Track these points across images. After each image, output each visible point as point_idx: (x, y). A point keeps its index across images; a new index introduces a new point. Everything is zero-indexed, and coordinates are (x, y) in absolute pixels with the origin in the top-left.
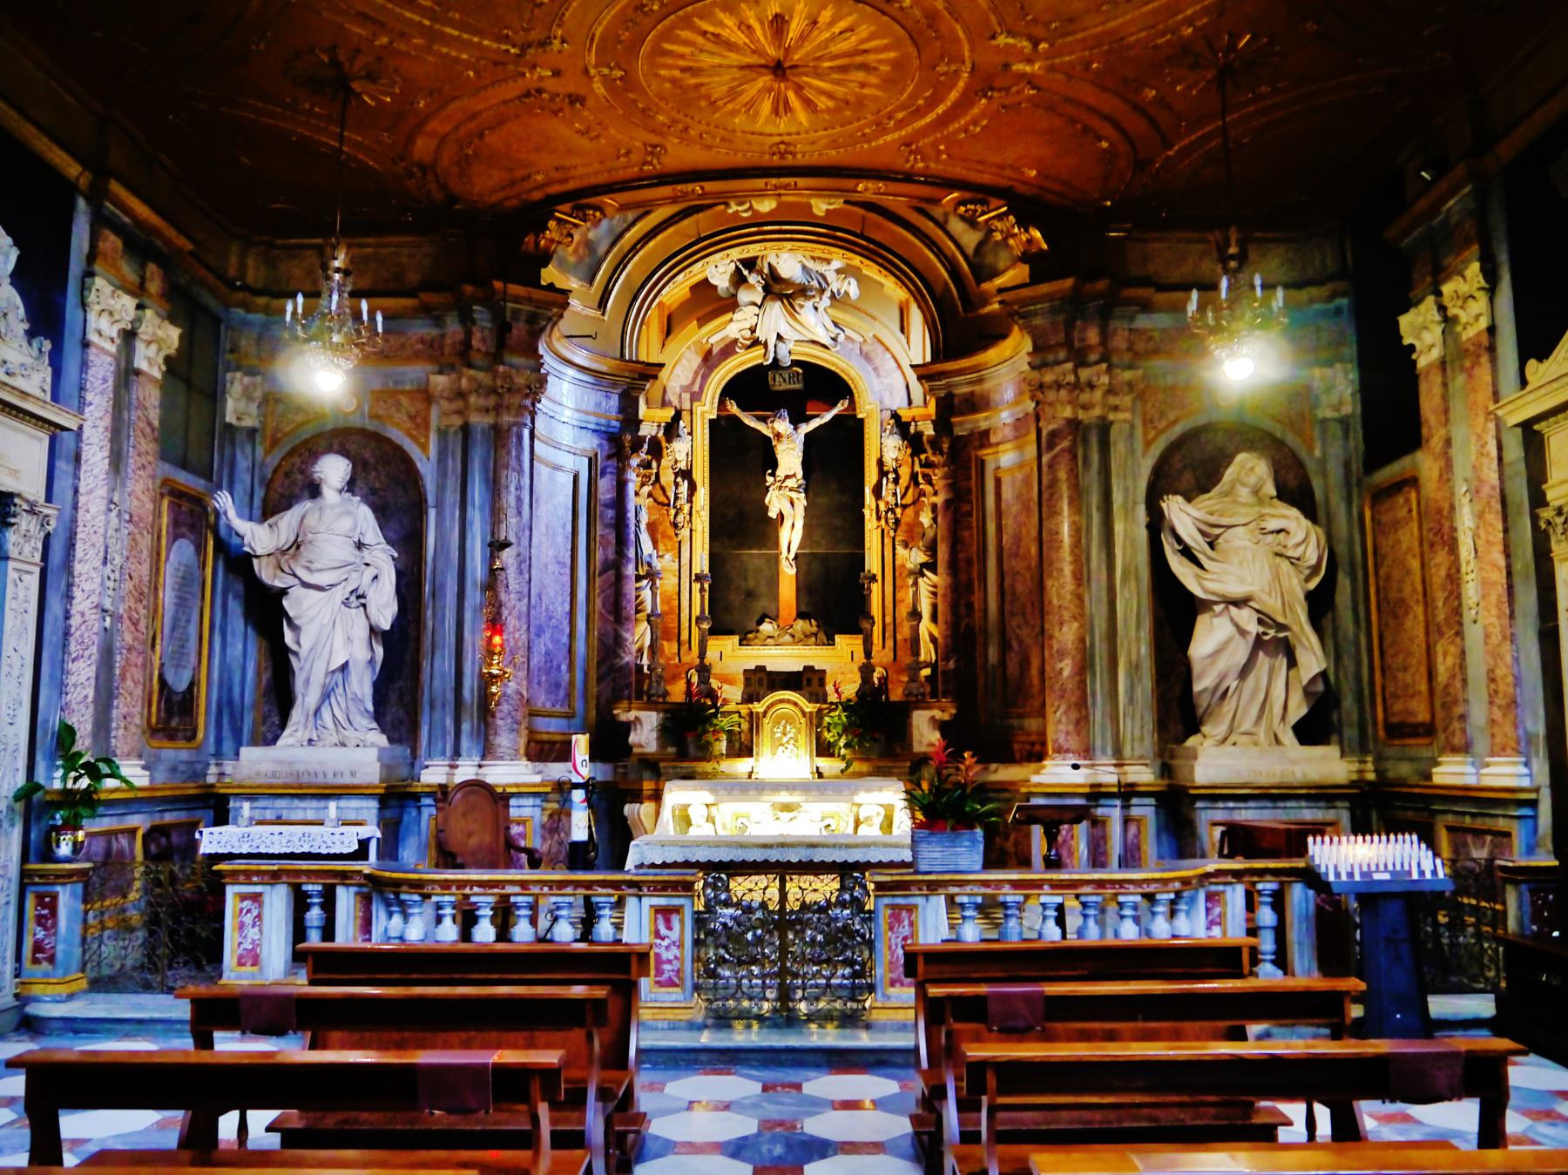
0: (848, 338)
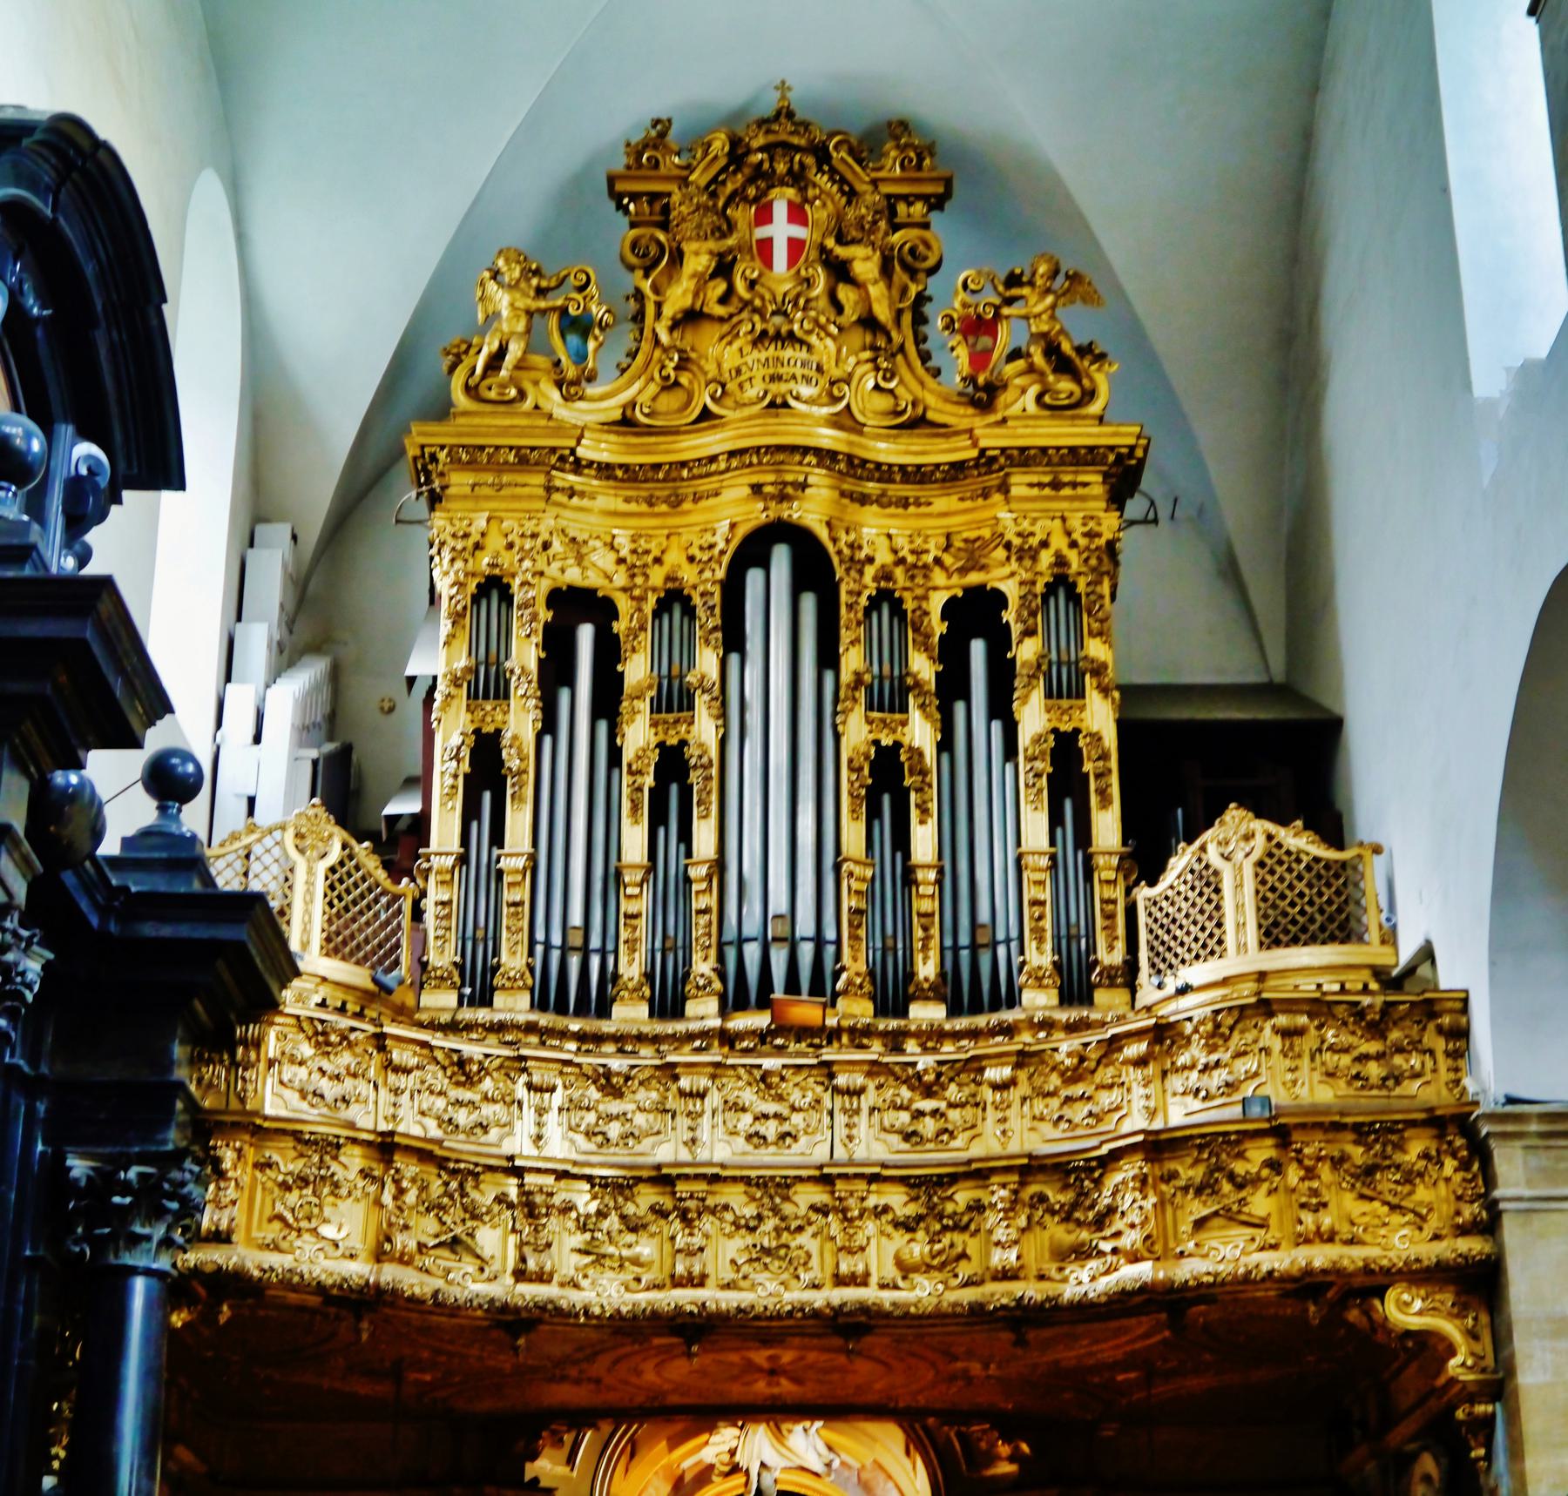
0: (843, 1463)
